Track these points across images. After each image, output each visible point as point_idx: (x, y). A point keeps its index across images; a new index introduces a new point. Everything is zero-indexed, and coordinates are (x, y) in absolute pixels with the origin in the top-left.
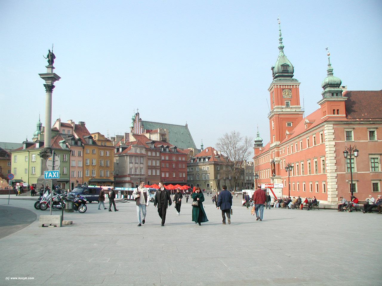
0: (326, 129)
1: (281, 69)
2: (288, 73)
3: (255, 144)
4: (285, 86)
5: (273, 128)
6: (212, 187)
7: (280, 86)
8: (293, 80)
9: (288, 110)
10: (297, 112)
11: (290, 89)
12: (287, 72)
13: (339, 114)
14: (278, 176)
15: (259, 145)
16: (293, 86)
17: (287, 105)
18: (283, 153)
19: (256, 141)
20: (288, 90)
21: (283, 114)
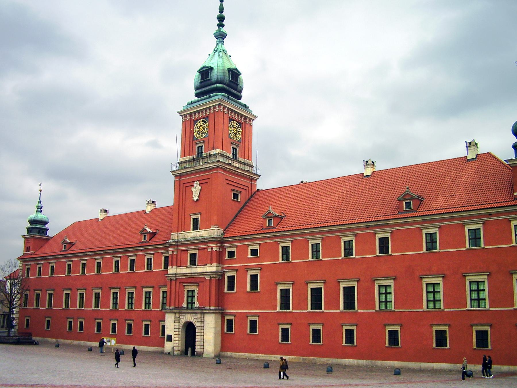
2: (236, 90)
3: (30, 230)
4: (236, 112)
5: (195, 198)
7: (229, 109)
8: (245, 106)
9: (235, 164)
10: (251, 173)
11: (240, 124)
14: (217, 308)
15: (41, 231)
16: (246, 118)
17: (235, 155)
18: (249, 256)
19: (32, 222)
21: (230, 172)
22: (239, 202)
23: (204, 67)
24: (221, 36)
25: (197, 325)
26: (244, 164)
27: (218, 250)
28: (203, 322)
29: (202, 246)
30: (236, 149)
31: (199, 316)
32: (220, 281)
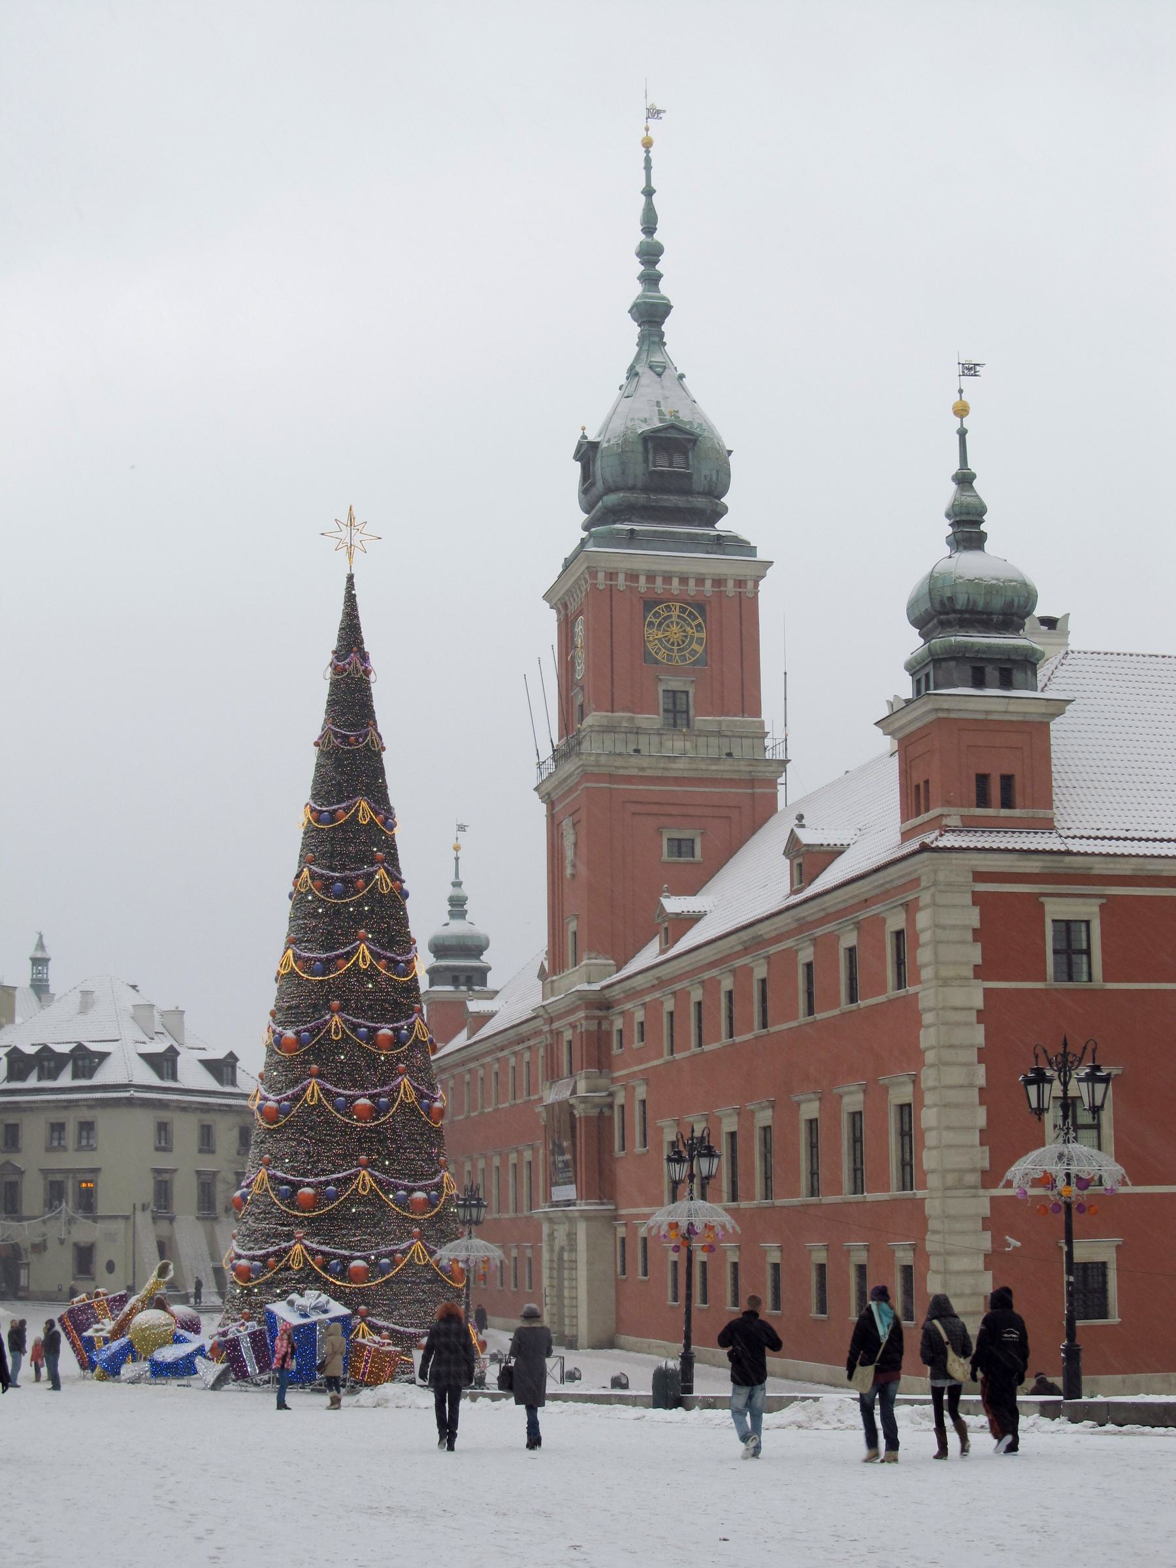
0: (925, 898)
1: (640, 458)
2: (688, 492)
6: (110, 1267)
9: (677, 744)
11: (701, 607)
12: (682, 484)
13: (1018, 798)
15: (462, 979)
16: (719, 582)
20: (683, 610)
22: (698, 863)
23: (580, 445)
24: (651, 316)
25: (566, 1256)
26: (719, 734)
27: (593, 1026)
28: (573, 1248)
29: (572, 1019)
30: (687, 693)
31: (566, 1226)
32: (601, 1123)
